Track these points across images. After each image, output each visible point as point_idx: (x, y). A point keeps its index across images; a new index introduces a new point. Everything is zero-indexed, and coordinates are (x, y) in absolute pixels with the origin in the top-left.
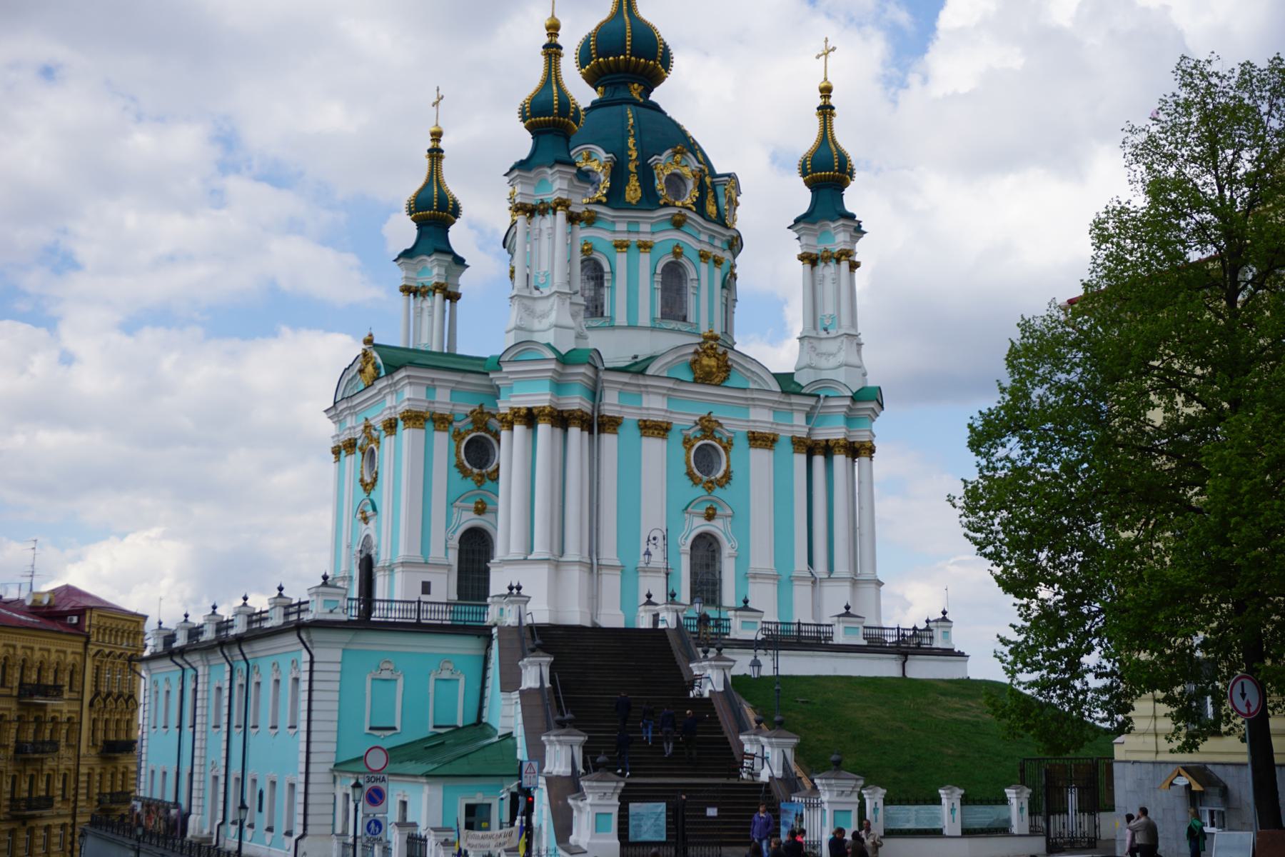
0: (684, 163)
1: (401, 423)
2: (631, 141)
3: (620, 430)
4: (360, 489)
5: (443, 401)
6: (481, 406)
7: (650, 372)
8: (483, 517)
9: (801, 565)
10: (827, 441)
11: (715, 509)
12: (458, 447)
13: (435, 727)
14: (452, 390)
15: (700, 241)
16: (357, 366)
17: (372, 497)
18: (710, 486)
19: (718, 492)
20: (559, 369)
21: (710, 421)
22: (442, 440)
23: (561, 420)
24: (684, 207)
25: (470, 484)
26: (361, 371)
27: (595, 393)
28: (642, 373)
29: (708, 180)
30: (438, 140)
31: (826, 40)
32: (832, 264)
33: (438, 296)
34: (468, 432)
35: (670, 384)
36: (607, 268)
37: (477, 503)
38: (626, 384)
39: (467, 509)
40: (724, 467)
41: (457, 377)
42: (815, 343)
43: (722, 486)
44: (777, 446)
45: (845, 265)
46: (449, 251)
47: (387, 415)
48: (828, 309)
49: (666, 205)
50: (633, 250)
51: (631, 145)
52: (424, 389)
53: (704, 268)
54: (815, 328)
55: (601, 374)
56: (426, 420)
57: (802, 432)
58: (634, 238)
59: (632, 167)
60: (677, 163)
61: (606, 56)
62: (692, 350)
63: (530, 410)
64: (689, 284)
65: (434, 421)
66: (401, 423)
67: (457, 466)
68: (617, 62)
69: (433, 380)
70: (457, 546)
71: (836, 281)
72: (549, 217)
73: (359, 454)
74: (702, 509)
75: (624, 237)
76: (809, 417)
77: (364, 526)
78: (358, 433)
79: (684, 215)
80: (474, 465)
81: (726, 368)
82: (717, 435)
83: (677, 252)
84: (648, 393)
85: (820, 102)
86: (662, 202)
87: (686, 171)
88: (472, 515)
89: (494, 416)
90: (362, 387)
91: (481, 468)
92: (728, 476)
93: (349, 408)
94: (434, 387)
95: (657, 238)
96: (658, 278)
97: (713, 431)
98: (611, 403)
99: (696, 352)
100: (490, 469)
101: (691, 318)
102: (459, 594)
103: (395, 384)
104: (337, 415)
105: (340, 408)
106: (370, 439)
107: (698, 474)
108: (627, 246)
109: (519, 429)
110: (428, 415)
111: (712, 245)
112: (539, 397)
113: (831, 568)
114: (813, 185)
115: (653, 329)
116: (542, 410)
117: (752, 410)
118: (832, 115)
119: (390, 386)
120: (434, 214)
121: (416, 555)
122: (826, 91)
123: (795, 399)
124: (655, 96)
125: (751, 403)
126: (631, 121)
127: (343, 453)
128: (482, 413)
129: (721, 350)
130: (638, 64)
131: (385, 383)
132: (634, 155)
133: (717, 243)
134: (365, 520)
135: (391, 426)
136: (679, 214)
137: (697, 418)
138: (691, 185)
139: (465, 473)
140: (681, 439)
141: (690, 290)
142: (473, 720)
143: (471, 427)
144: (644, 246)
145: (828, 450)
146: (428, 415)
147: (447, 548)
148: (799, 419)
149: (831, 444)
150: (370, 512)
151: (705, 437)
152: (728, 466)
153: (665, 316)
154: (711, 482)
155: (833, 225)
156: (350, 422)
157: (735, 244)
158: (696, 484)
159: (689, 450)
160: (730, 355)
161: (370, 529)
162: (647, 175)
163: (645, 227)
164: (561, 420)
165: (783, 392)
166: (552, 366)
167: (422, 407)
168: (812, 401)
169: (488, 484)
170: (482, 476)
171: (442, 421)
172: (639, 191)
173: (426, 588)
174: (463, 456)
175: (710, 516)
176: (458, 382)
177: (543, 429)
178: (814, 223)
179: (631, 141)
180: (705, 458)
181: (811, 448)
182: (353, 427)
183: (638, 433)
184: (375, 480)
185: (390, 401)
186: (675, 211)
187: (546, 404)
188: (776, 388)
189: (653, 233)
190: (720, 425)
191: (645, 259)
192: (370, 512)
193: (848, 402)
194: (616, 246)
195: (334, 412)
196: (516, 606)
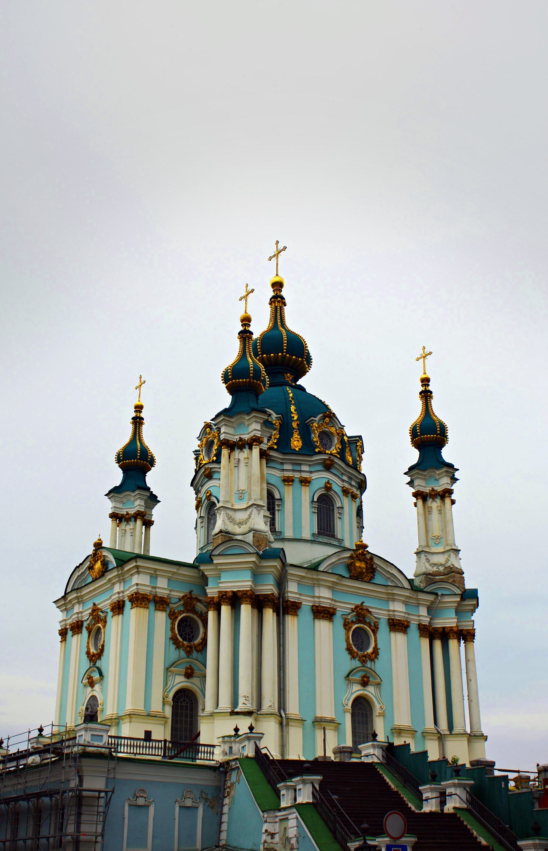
1: (128, 604)
2: (293, 408)
3: (300, 613)
5: (162, 586)
6: (190, 592)
7: (321, 568)
8: (191, 680)
9: (430, 724)
11: (368, 678)
15: (343, 481)
16: (87, 564)
17: (97, 665)
18: (364, 659)
19: (369, 664)
20: (257, 562)
21: (362, 609)
24: (331, 454)
26: (91, 568)
27: (281, 583)
29: (345, 438)
30: (140, 412)
31: (424, 348)
32: (438, 500)
33: (139, 522)
34: (181, 612)
35: (333, 579)
36: (277, 496)
37: (187, 668)
43: (372, 660)
44: (409, 631)
45: (448, 501)
46: (148, 489)
47: (115, 598)
49: (319, 453)
50: (297, 484)
51: (293, 410)
52: (149, 577)
55: (287, 568)
56: (149, 601)
57: (426, 620)
59: (294, 425)
60: (327, 424)
61: (268, 353)
62: (349, 555)
64: (336, 511)
66: (128, 604)
67: (171, 638)
68: (276, 357)
69: (156, 570)
71: (440, 512)
73: (85, 632)
74: (357, 677)
75: (290, 474)
77: (89, 689)
78: (86, 616)
79: (332, 461)
80: (184, 639)
82: (368, 620)
83: (328, 487)
84: (319, 586)
86: (317, 450)
87: (333, 430)
88: (182, 679)
89: (200, 601)
90: (90, 579)
91: (190, 641)
92: (376, 651)
93: (77, 598)
95: (314, 476)
97: (364, 617)
98: (293, 590)
99: (351, 557)
100: (198, 641)
103: (123, 574)
105: (69, 599)
107: (355, 649)
108: (292, 481)
109: (225, 610)
110: (151, 598)
111: (351, 485)
113: (451, 726)
114: (417, 444)
115: (312, 542)
116: (245, 593)
118: (431, 397)
120: (136, 462)
122: (425, 381)
123: (421, 596)
124: (300, 382)
125: (392, 598)
126: (291, 395)
127: (70, 633)
128: (191, 598)
129: (368, 556)
130: (290, 359)
131: (116, 573)
132: (296, 418)
133: (353, 483)
134: (92, 684)
137: (353, 607)
138: (336, 440)
139: (178, 645)
140: (342, 622)
141: (336, 515)
144: (305, 482)
145: (443, 635)
146: (151, 598)
147: (164, 704)
148: (423, 611)
150: (96, 676)
153: (319, 533)
154: (365, 656)
155: (438, 472)
157: (362, 485)
160: (376, 561)
161: (97, 691)
162: (305, 432)
163: (305, 468)
164: (259, 603)
167: (146, 590)
168: (431, 598)
169: (195, 654)
170: (190, 647)
171: (161, 603)
172: (300, 442)
174: (177, 632)
175: (365, 683)
176: (174, 573)
177: (246, 610)
179: (293, 408)
181: (431, 633)
182: (82, 611)
184: (102, 651)
185: (117, 588)
187: (249, 589)
188: (406, 585)
189: (311, 472)
190: (370, 612)
192: (96, 676)
195: (63, 603)
196: (252, 742)
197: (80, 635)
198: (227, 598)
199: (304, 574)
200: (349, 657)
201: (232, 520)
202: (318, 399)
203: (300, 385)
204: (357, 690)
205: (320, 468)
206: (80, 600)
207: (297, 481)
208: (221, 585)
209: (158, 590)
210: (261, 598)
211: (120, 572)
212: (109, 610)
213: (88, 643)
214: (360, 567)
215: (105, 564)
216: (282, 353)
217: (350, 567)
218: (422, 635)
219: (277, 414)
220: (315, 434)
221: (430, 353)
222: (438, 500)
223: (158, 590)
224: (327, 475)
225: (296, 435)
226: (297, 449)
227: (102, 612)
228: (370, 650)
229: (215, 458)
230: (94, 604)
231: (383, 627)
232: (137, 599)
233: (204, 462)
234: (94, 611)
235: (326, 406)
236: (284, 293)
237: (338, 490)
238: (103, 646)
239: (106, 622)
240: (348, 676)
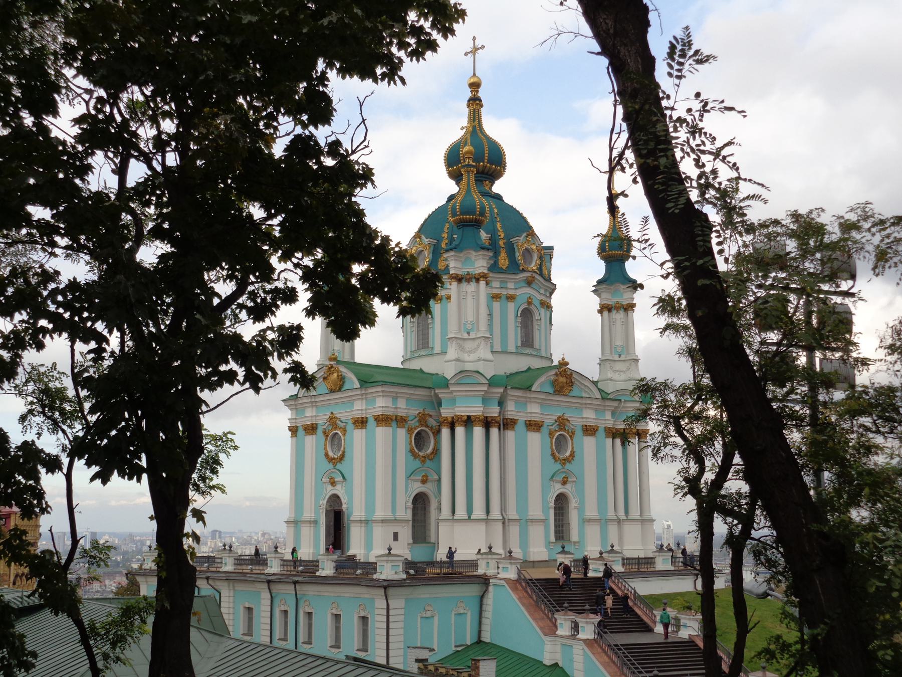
2: (499, 226)
3: (517, 427)
4: (325, 462)
5: (402, 407)
12: (410, 438)
13: (456, 646)
17: (337, 467)
22: (402, 433)
23: (487, 424)
25: (417, 463)
26: (325, 378)
27: (501, 403)
28: (528, 388)
35: (544, 397)
38: (519, 396)
39: (416, 481)
41: (411, 391)
43: (570, 462)
47: (358, 415)
48: (619, 342)
53: (542, 311)
54: (611, 354)
57: (610, 424)
58: (504, 292)
59: (501, 243)
62: (553, 372)
63: (469, 417)
66: (371, 422)
69: (397, 393)
72: (473, 284)
74: (560, 478)
77: (330, 487)
79: (534, 277)
84: (530, 402)
87: (534, 247)
88: (419, 484)
92: (572, 455)
93: (312, 402)
96: (519, 320)
98: (512, 410)
99: (556, 374)
101: (537, 345)
102: (414, 538)
103: (366, 394)
108: (500, 298)
112: (475, 409)
113: (627, 512)
115: (516, 353)
116: (478, 417)
117: (584, 411)
119: (362, 395)
121: (389, 515)
123: (608, 403)
125: (585, 406)
126: (496, 211)
127: (301, 432)
131: (359, 392)
135: (361, 423)
138: (535, 257)
141: (535, 327)
142: (475, 640)
143: (417, 424)
144: (511, 298)
148: (608, 416)
150: (339, 478)
151: (560, 430)
156: (309, 412)
160: (574, 376)
163: (511, 285)
164: (487, 424)
165: (603, 398)
166: (485, 388)
167: (390, 412)
168: (616, 404)
171: (401, 421)
173: (396, 537)
175: (564, 483)
177: (478, 431)
178: (612, 284)
179: (499, 226)
180: (560, 443)
181: (613, 433)
184: (343, 456)
191: (511, 307)
192: (339, 478)
193: (638, 405)
194: (493, 297)
201: (462, 349)
203: (498, 195)
204: (558, 489)
205: (524, 284)
207: (504, 297)
210: (489, 420)
212: (350, 422)
213: (325, 445)
215: (342, 379)
217: (554, 383)
218: (607, 436)
222: (622, 312)
224: (528, 290)
225: (503, 254)
226: (504, 268)
228: (568, 454)
231: (579, 432)
234: (331, 418)
235: (524, 218)
236: (481, 94)
237: (537, 303)
238: (344, 452)
240: (552, 477)
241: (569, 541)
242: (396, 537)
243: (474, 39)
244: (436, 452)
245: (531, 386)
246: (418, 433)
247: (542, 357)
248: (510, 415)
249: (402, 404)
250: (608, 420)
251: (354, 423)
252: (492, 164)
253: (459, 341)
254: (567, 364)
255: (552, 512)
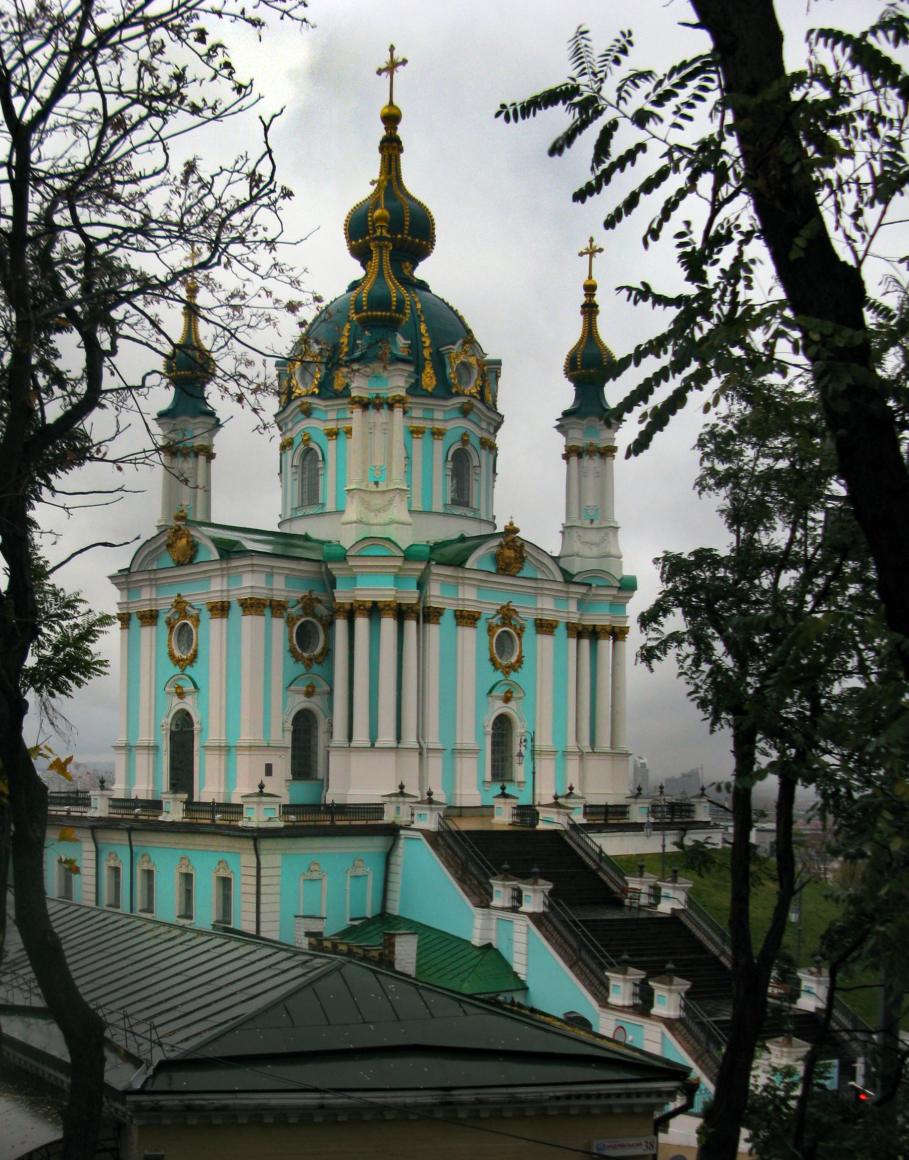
0: (470, 352)
2: (423, 328)
3: (442, 619)
8: (311, 699)
10: (594, 626)
13: (352, 920)
14: (287, 577)
19: (513, 676)
22: (279, 625)
23: (401, 613)
24: (471, 395)
25: (300, 668)
37: (308, 686)
39: (298, 692)
40: (517, 653)
42: (581, 532)
43: (515, 671)
44: (556, 631)
47: (217, 598)
48: (591, 501)
49: (458, 394)
51: (423, 331)
52: (263, 577)
53: (484, 453)
54: (580, 518)
56: (264, 606)
58: (428, 425)
59: (426, 353)
60: (466, 352)
63: (375, 603)
65: (271, 606)
66: (236, 610)
69: (272, 567)
70: (291, 728)
74: (500, 692)
76: (580, 603)
79: (472, 405)
81: (521, 559)
82: (513, 623)
84: (463, 584)
85: (583, 300)
86: (454, 390)
87: (473, 360)
92: (520, 661)
94: (272, 574)
95: (450, 426)
97: (510, 618)
98: (437, 595)
99: (501, 545)
102: (293, 773)
103: (228, 568)
104: (127, 583)
106: (184, 614)
108: (423, 433)
109: (362, 624)
110: (268, 603)
116: (387, 605)
119: (222, 569)
121: (258, 738)
125: (539, 592)
126: (419, 306)
131: (218, 566)
132: (427, 344)
136: (469, 403)
140: (486, 626)
142: (378, 911)
143: (301, 613)
144: (438, 434)
145: (593, 634)
148: (573, 606)
149: (598, 629)
151: (504, 625)
152: (521, 652)
158: (496, 669)
159: (491, 637)
160: (527, 548)
163: (439, 415)
166: (399, 564)
167: (262, 594)
168: (583, 590)
169: (315, 668)
170: (310, 660)
171: (277, 608)
173: (269, 770)
177: (388, 624)
179: (423, 328)
181: (579, 632)
183: (454, 622)
184: (195, 656)
186: (465, 400)
188: (560, 578)
189: (446, 421)
190: (516, 613)
191: (439, 447)
193: (614, 592)
197: (154, 628)
198: (365, 609)
199: (449, 573)
200: (492, 668)
201: (368, 507)
202: (447, 304)
203: (422, 282)
204: (499, 708)
205: (457, 414)
206: (154, 583)
207: (427, 431)
208: (357, 592)
209: (275, 592)
210: (404, 608)
211: (224, 566)
212: (205, 609)
214: (509, 557)
215: (194, 547)
216: (402, 234)
217: (497, 558)
219: (406, 339)
220: (452, 367)
221: (601, 250)
222: (597, 458)
223: (275, 592)
224: (464, 424)
225: (429, 370)
226: (430, 389)
227: (192, 607)
228: (514, 659)
229: (317, 391)
230: (179, 595)
231: (530, 629)
232: (252, 606)
233: (298, 391)
235: (460, 319)
236: (402, 131)
237: (475, 442)
238: (196, 651)
239: (198, 621)
241: (511, 781)
242: (269, 770)
243: (392, 49)
244: (328, 652)
245: (465, 561)
246: (302, 626)
247: (481, 520)
248: (434, 603)
249: (279, 583)
250: (571, 612)
251: (211, 610)
252: (414, 237)
253: (362, 495)
254: (517, 531)
255: (488, 740)
